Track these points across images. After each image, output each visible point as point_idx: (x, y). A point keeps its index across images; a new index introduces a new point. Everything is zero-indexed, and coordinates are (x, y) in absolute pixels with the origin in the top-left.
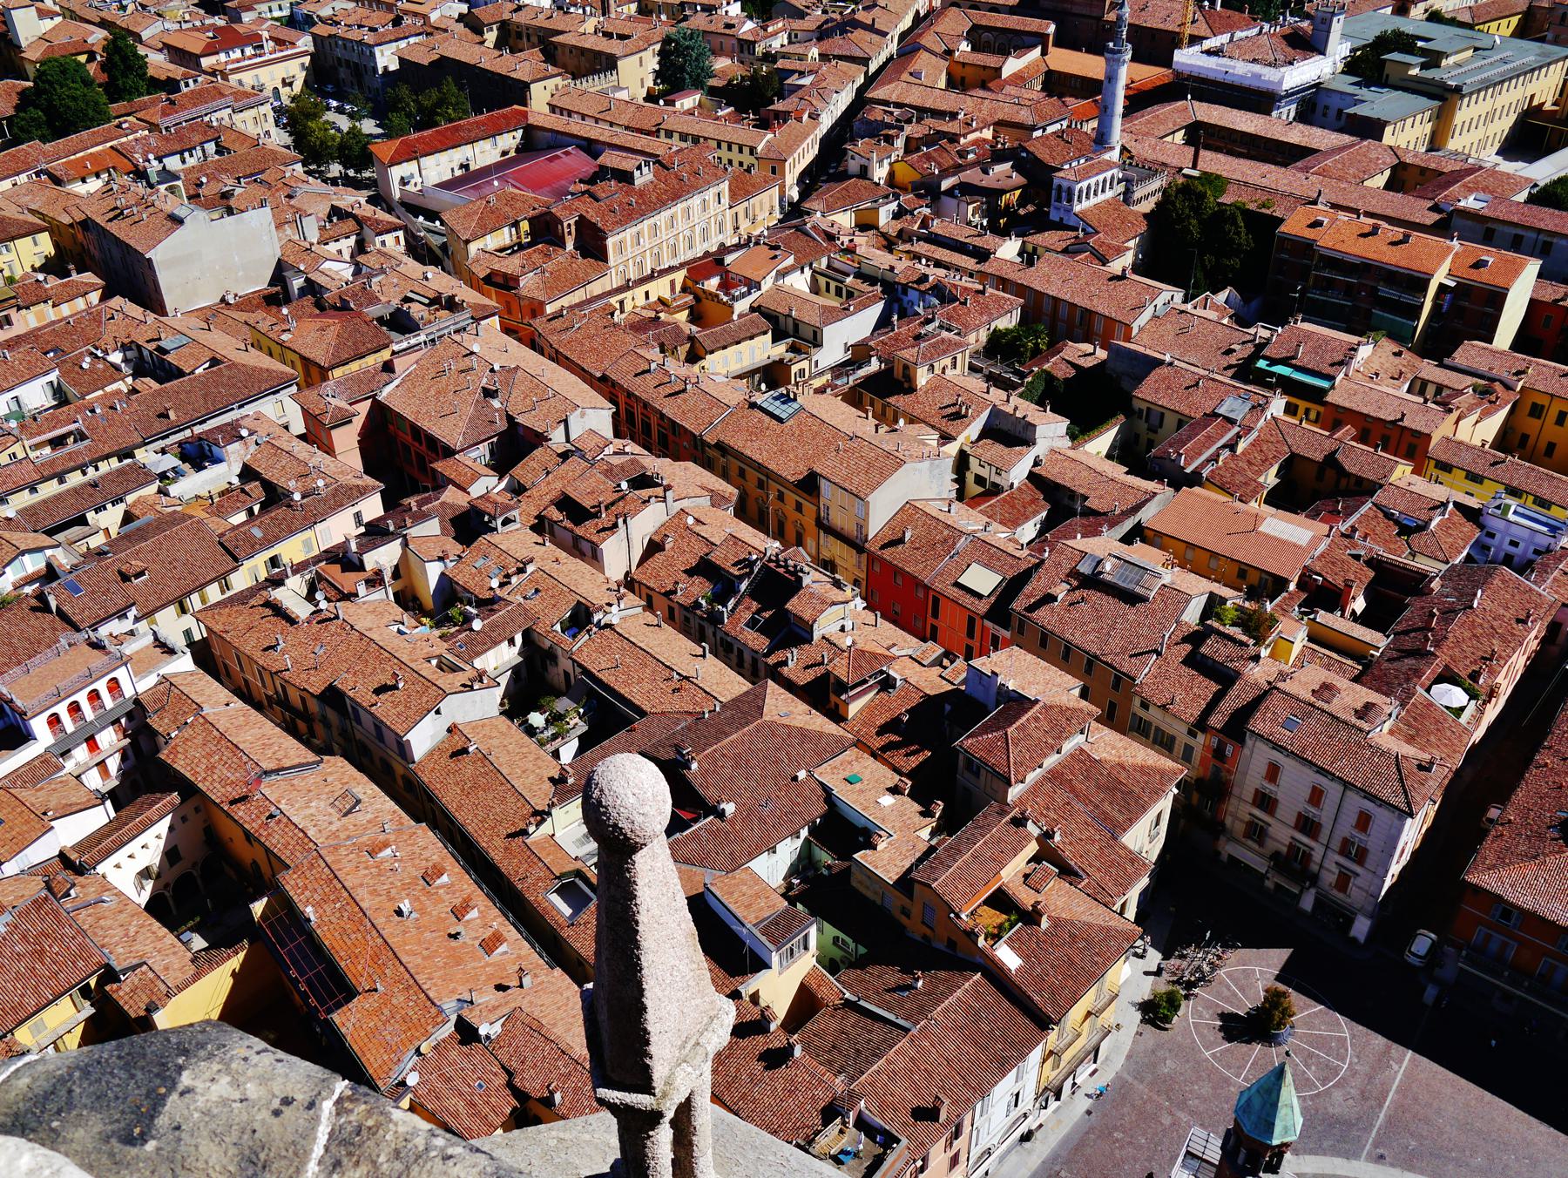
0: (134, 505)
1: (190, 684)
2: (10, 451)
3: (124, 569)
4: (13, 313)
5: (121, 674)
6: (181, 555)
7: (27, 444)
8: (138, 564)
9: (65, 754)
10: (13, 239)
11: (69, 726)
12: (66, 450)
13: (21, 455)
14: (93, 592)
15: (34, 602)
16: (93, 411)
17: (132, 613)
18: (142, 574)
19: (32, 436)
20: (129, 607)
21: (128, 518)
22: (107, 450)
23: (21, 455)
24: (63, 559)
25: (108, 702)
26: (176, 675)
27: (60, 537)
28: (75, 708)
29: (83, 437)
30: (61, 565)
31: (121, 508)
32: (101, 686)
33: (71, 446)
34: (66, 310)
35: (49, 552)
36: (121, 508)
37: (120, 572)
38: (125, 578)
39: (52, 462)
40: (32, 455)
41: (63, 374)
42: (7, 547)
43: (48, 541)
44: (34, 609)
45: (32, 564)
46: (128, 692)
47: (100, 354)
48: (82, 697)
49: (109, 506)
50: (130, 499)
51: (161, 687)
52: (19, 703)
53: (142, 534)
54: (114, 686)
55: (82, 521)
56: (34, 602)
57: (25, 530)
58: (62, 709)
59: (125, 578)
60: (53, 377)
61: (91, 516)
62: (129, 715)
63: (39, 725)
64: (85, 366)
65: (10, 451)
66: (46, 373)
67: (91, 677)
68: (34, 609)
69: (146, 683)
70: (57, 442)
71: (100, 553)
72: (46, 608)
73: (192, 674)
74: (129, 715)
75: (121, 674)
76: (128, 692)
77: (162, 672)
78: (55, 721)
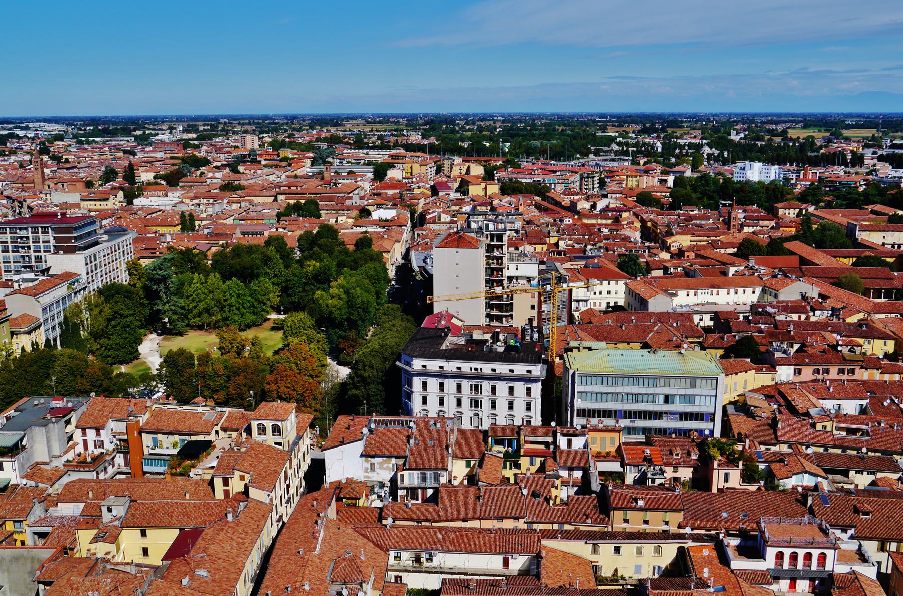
0: (881, 479)
1: (869, 585)
2: (824, 424)
3: (858, 505)
4: (857, 369)
5: (830, 553)
6: (897, 517)
7: (835, 425)
8: (867, 507)
9: (776, 579)
10: (874, 338)
11: (786, 566)
12: (854, 437)
13: (829, 429)
14: (834, 508)
15: (799, 497)
16: (880, 424)
17: (851, 532)
18: (867, 513)
19: (839, 422)
20: (851, 527)
21: (873, 483)
22: (878, 447)
23: (829, 429)
24: (825, 485)
25: (814, 567)
26: (862, 575)
27: (830, 476)
28: (794, 557)
29: (868, 435)
30: (822, 489)
31: (872, 478)
32: (815, 553)
33: (858, 436)
34: (887, 377)
35: (820, 479)
36: (872, 478)
37: (855, 506)
38: (857, 511)
39: (843, 440)
40: (835, 432)
41: (870, 403)
42: (799, 466)
43: (823, 474)
44: (797, 500)
45: (808, 481)
46: (828, 568)
47: (896, 401)
48: (801, 553)
49: (865, 473)
50: (880, 475)
51: (849, 576)
52: (767, 535)
53: (879, 494)
54: (823, 557)
55: (846, 474)
56: (799, 497)
57: (813, 462)
58: (787, 552)
59: (857, 511)
60: (864, 403)
61: (852, 473)
62: (822, 580)
63: (771, 553)
64: (885, 404)
65: (824, 424)
66: (862, 399)
67: (812, 545)
68: (797, 500)
69: (842, 569)
70: (851, 432)
71: (849, 492)
72: (805, 503)
73: (872, 581)
74: (822, 580)
75: (830, 553)
76: (828, 568)
77: (855, 568)
78: (780, 557)
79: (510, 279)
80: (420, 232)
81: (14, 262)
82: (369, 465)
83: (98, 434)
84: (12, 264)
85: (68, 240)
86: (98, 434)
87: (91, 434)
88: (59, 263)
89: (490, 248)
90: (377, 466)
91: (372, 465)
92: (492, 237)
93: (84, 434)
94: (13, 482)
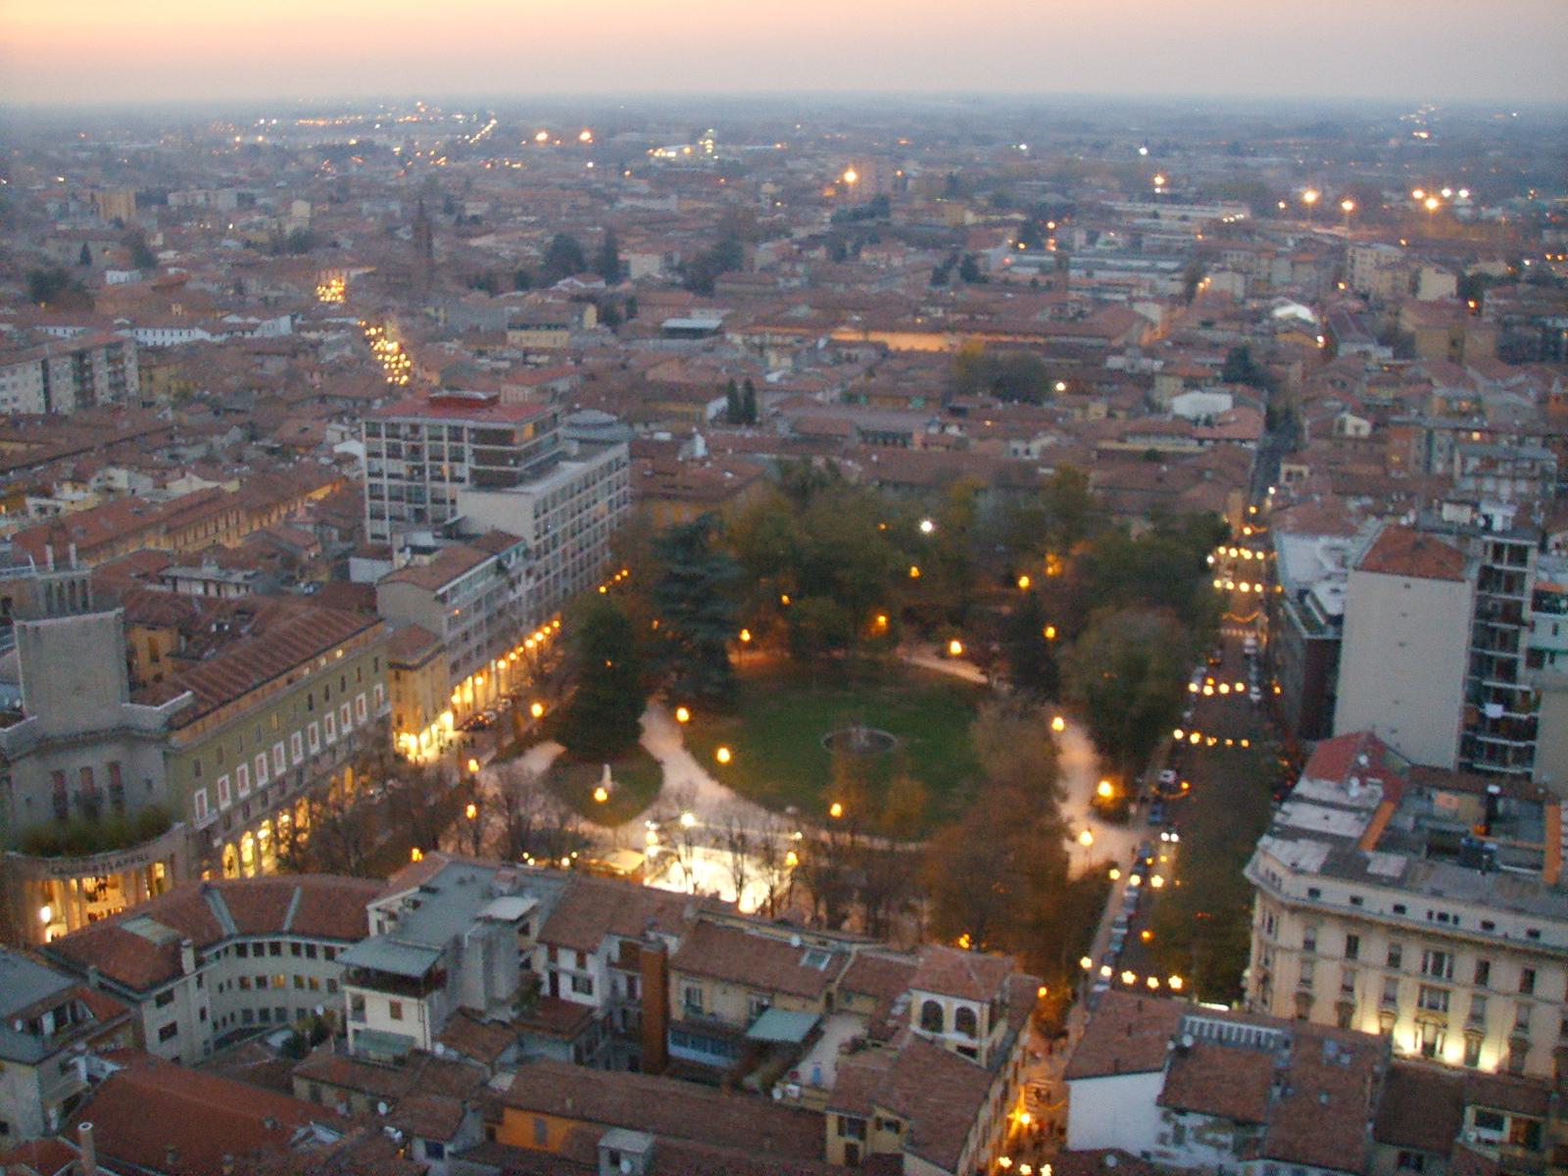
79: (1536, 657)
80: (1295, 468)
81: (391, 498)
82: (1168, 1129)
83: (581, 963)
84: (386, 503)
85: (502, 458)
86: (581, 963)
87: (567, 961)
88: (481, 510)
89: (1487, 578)
90: (1189, 1135)
91: (1179, 1131)
92: (1498, 550)
93: (553, 958)
94: (420, 1044)
